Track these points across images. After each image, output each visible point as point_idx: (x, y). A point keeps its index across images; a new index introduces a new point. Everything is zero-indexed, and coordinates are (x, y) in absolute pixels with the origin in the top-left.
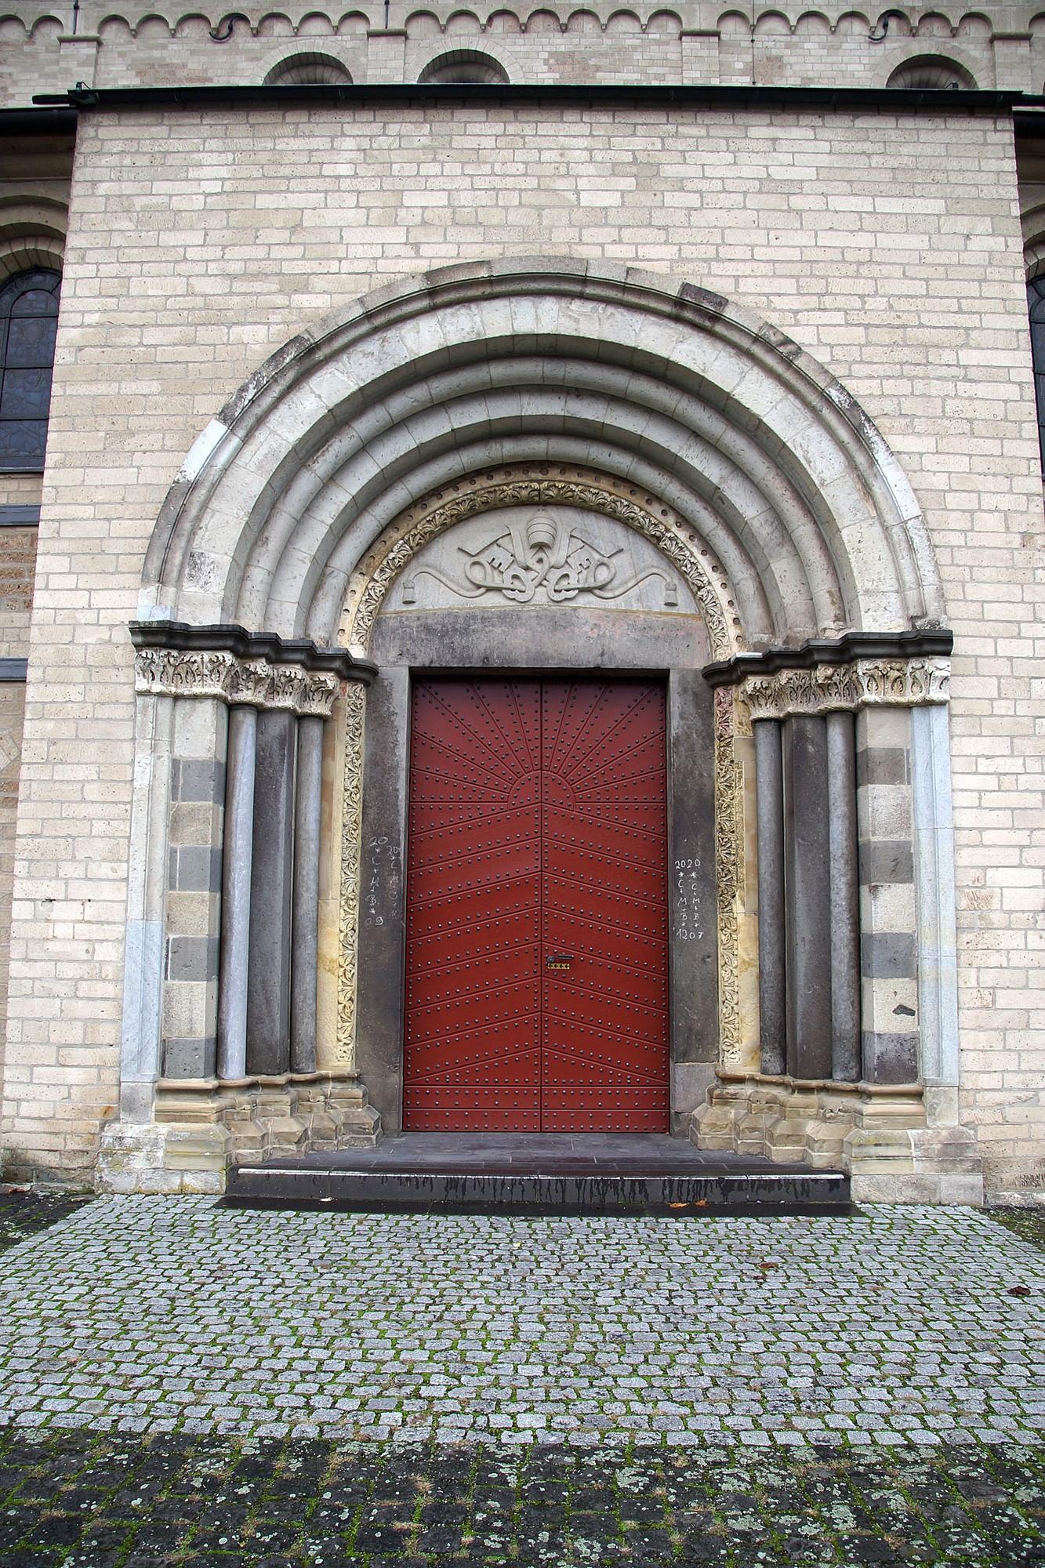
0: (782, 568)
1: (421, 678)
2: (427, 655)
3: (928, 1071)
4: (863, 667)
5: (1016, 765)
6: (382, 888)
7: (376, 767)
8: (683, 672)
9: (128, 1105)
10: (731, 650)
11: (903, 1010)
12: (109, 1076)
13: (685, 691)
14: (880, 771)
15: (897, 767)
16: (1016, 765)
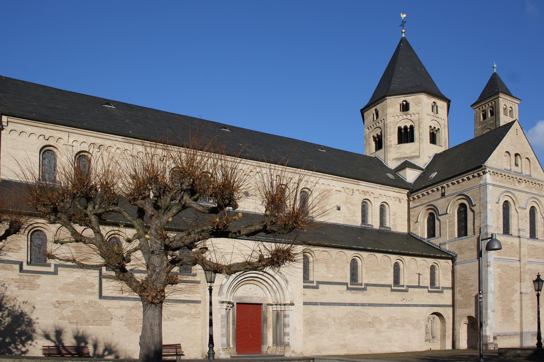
0: (278, 294)
1: (237, 303)
2: (238, 302)
3: (290, 345)
4: (286, 306)
5: (298, 316)
6: (234, 327)
7: (233, 313)
8: (265, 304)
9: (220, 350)
10: (271, 302)
11: (288, 339)
12: (217, 347)
13: (265, 306)
14: (287, 317)
15: (288, 316)
16: (298, 316)
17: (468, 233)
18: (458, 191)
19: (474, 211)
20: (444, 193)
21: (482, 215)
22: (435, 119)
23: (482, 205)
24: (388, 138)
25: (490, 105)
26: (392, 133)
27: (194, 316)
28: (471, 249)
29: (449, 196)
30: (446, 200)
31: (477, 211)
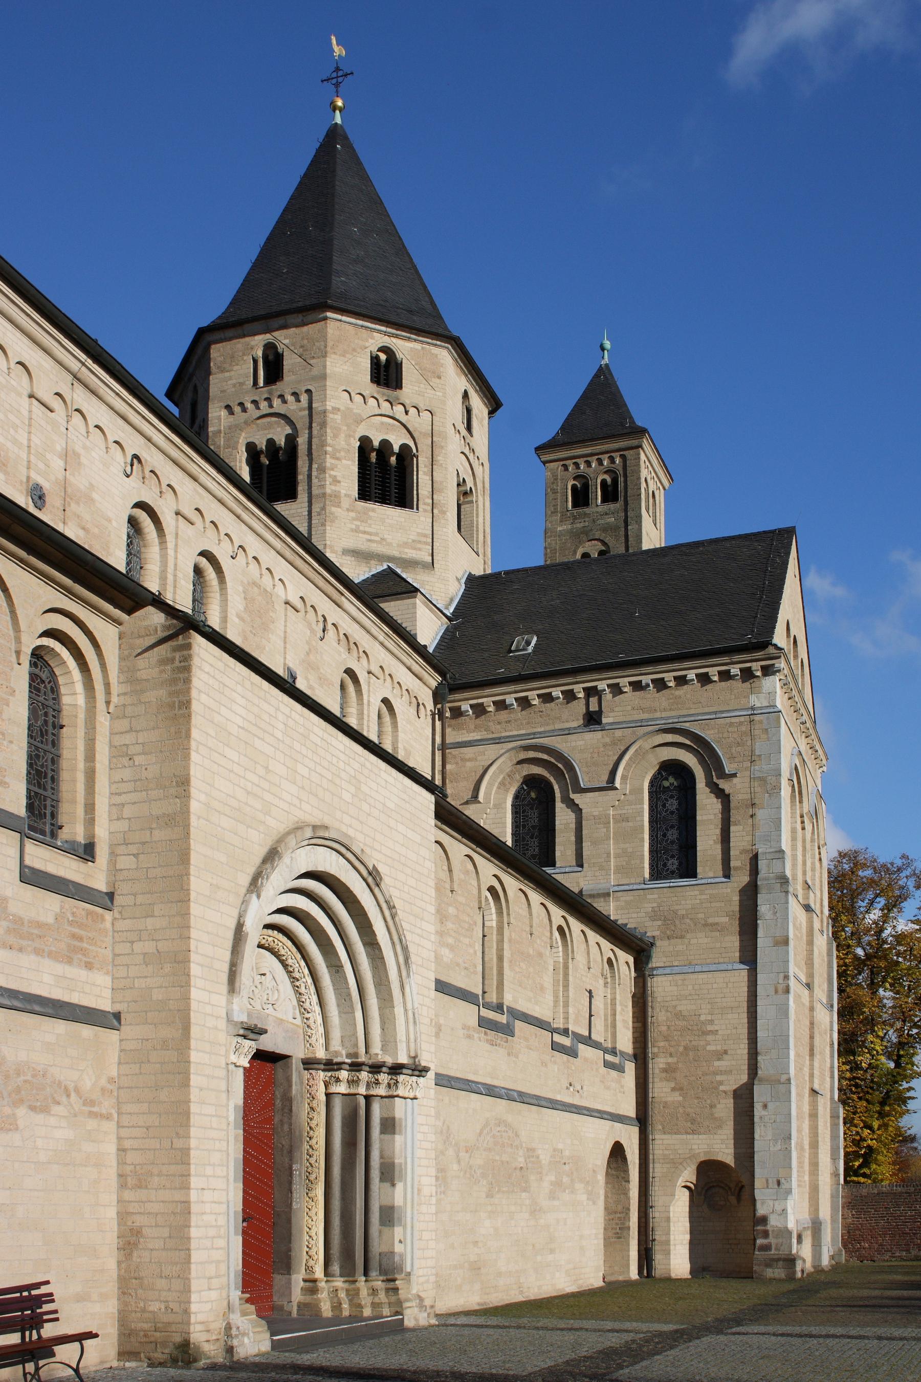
17: (699, 870)
18: (658, 715)
19: (729, 795)
20: (600, 712)
21: (761, 814)
22: (467, 451)
23: (763, 780)
24: (328, 465)
25: (605, 463)
26: (343, 454)
27: (92, 1103)
28: (712, 925)
29: (616, 726)
30: (608, 740)
31: (741, 797)
